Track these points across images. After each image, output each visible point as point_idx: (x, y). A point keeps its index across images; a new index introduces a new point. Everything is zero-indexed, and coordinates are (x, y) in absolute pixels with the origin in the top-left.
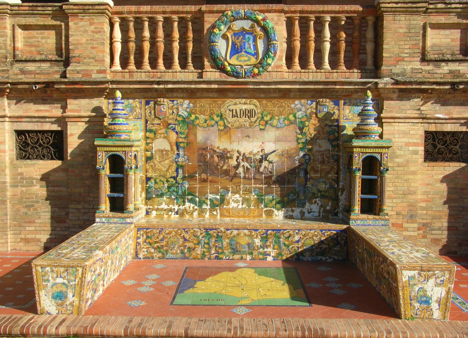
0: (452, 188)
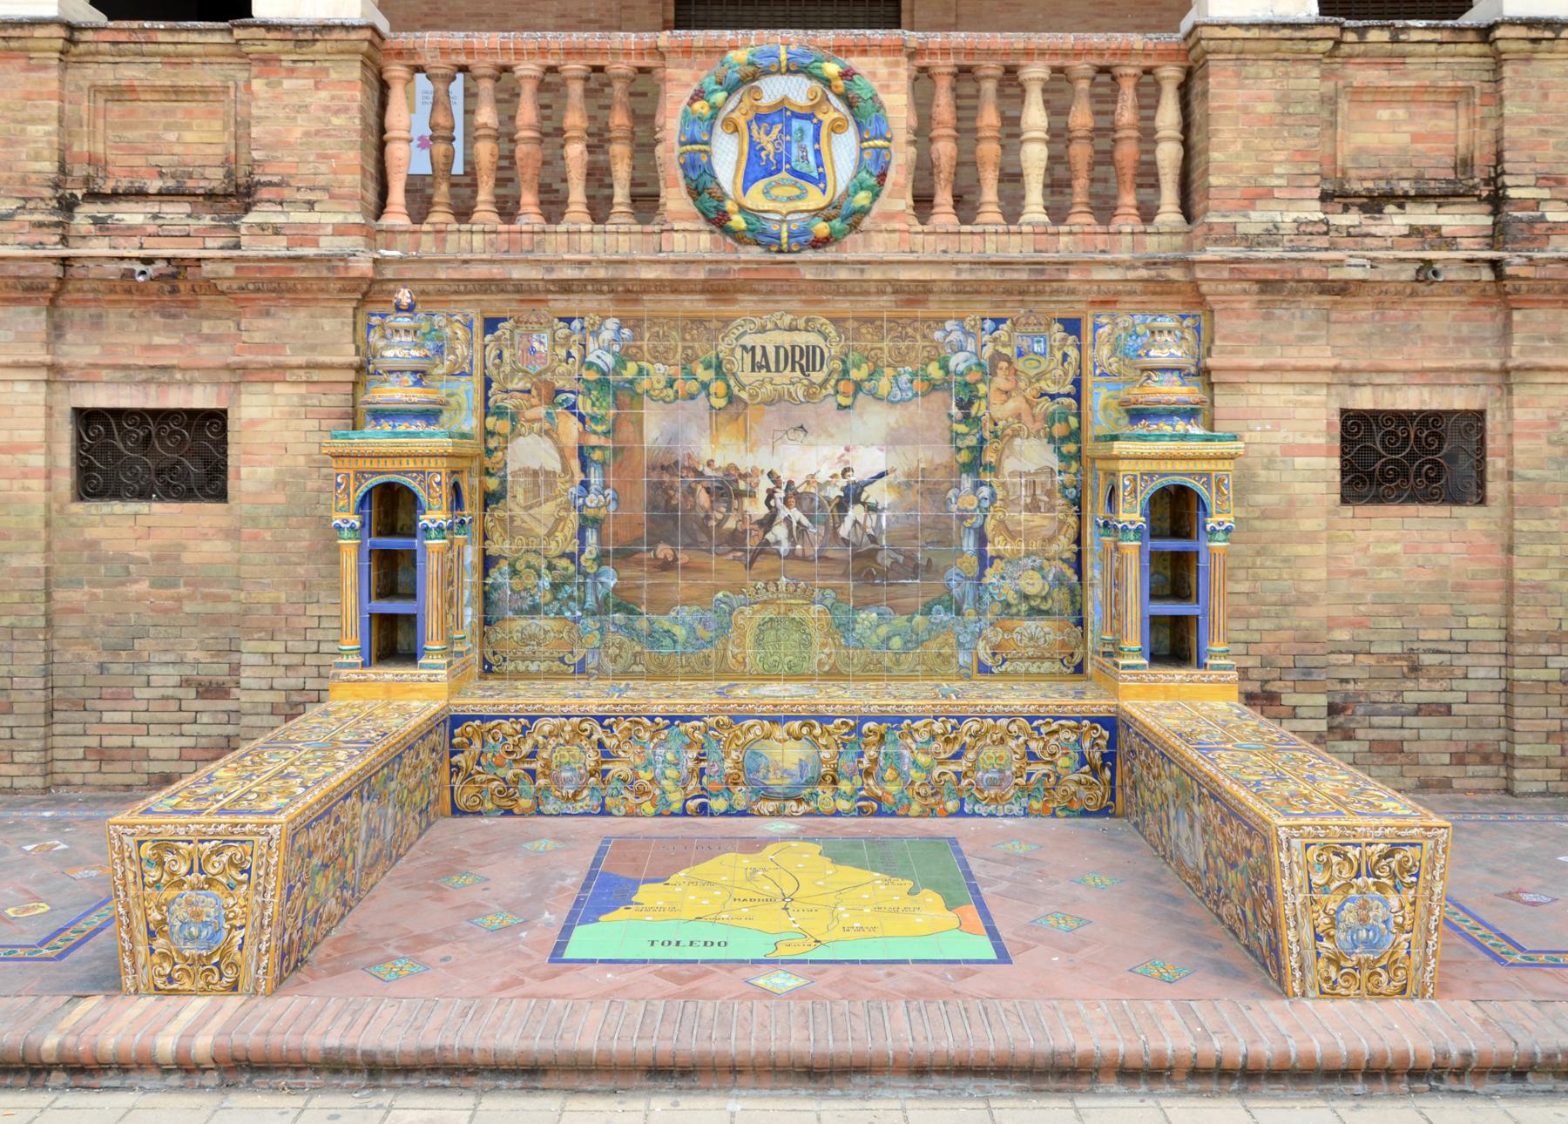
0: (1429, 583)
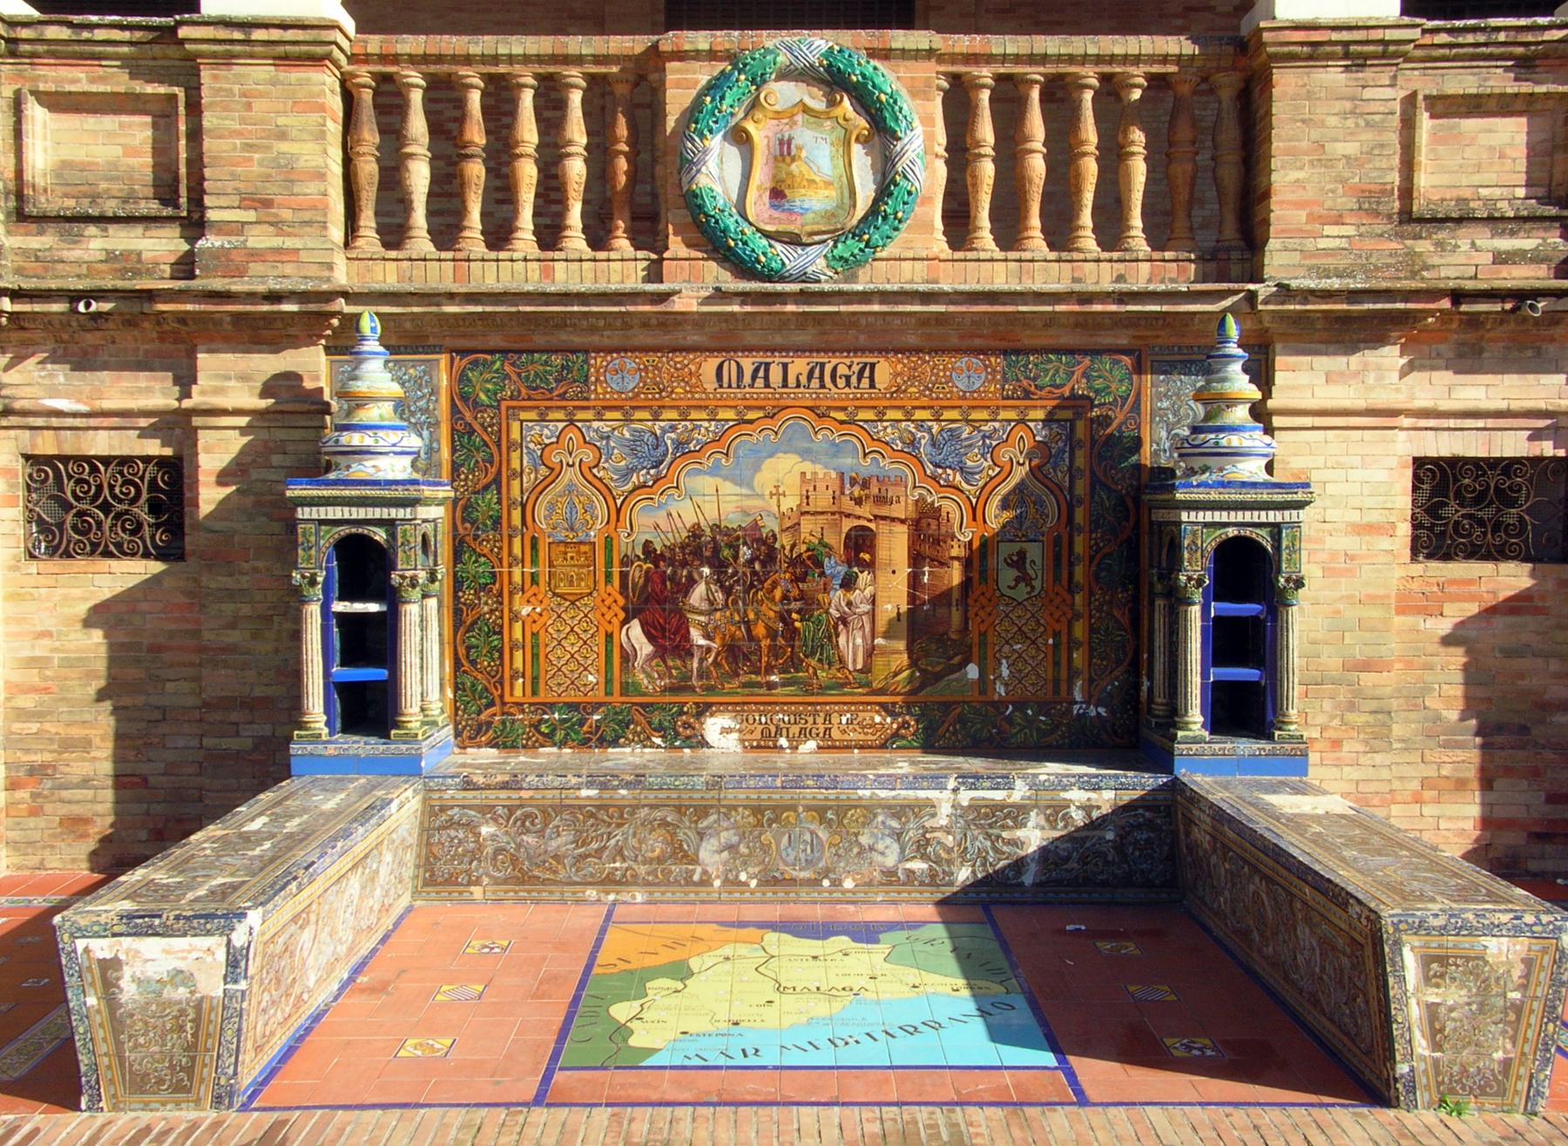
0: (123, 644)
